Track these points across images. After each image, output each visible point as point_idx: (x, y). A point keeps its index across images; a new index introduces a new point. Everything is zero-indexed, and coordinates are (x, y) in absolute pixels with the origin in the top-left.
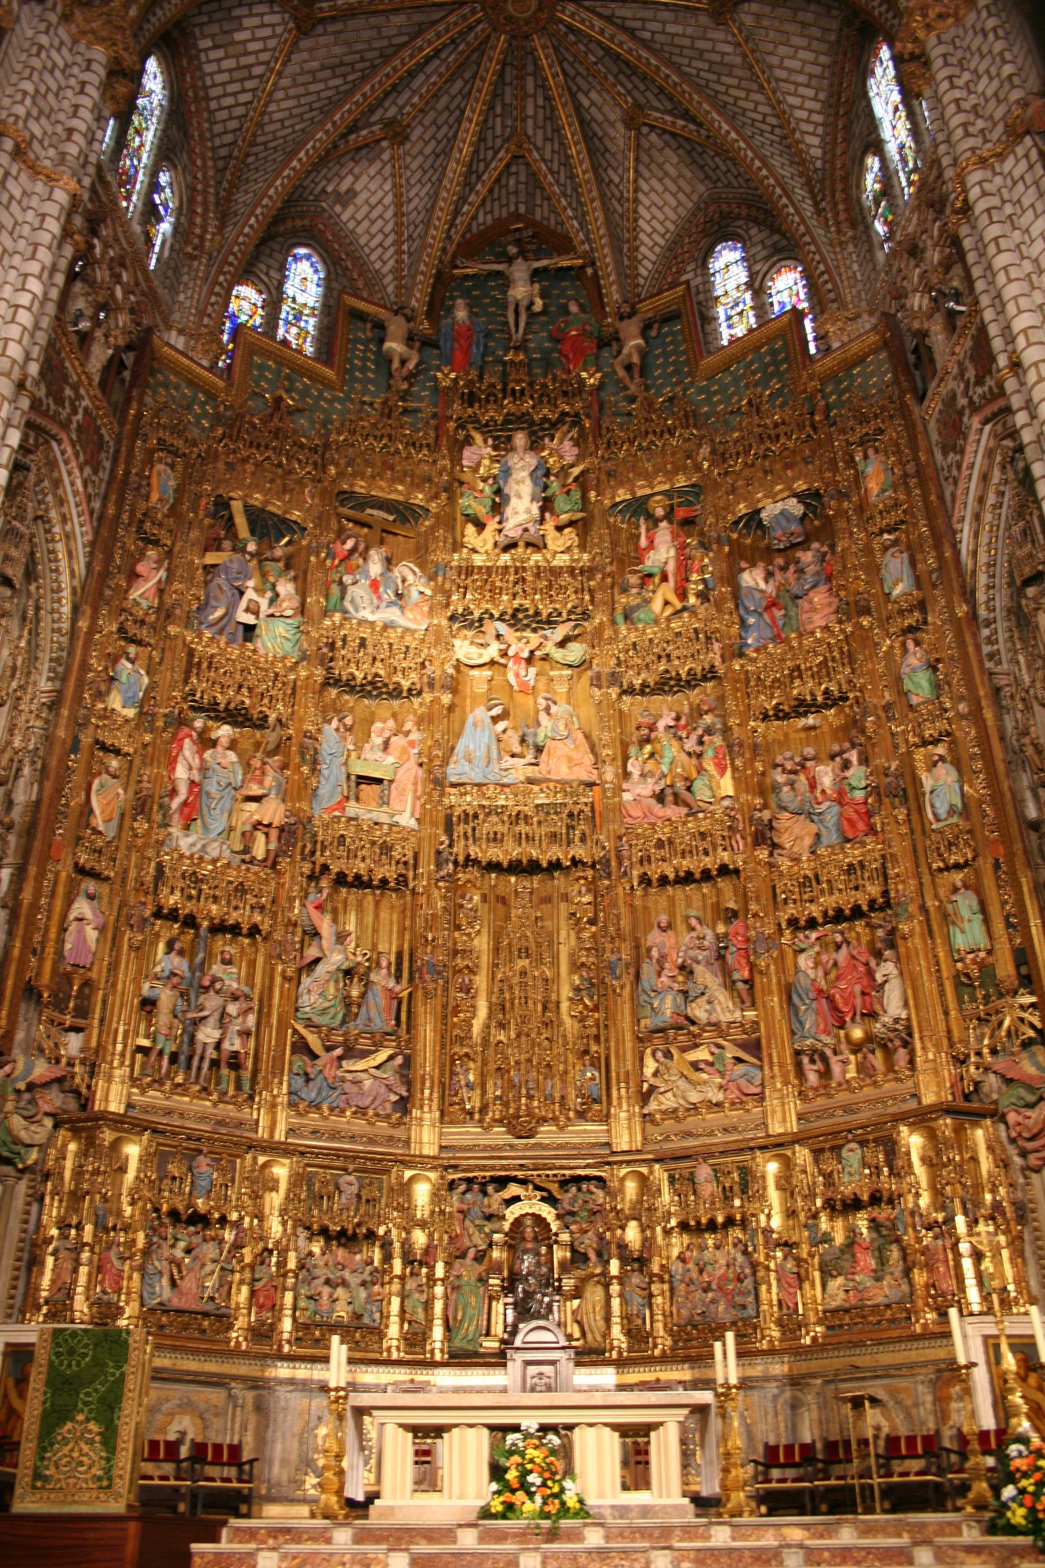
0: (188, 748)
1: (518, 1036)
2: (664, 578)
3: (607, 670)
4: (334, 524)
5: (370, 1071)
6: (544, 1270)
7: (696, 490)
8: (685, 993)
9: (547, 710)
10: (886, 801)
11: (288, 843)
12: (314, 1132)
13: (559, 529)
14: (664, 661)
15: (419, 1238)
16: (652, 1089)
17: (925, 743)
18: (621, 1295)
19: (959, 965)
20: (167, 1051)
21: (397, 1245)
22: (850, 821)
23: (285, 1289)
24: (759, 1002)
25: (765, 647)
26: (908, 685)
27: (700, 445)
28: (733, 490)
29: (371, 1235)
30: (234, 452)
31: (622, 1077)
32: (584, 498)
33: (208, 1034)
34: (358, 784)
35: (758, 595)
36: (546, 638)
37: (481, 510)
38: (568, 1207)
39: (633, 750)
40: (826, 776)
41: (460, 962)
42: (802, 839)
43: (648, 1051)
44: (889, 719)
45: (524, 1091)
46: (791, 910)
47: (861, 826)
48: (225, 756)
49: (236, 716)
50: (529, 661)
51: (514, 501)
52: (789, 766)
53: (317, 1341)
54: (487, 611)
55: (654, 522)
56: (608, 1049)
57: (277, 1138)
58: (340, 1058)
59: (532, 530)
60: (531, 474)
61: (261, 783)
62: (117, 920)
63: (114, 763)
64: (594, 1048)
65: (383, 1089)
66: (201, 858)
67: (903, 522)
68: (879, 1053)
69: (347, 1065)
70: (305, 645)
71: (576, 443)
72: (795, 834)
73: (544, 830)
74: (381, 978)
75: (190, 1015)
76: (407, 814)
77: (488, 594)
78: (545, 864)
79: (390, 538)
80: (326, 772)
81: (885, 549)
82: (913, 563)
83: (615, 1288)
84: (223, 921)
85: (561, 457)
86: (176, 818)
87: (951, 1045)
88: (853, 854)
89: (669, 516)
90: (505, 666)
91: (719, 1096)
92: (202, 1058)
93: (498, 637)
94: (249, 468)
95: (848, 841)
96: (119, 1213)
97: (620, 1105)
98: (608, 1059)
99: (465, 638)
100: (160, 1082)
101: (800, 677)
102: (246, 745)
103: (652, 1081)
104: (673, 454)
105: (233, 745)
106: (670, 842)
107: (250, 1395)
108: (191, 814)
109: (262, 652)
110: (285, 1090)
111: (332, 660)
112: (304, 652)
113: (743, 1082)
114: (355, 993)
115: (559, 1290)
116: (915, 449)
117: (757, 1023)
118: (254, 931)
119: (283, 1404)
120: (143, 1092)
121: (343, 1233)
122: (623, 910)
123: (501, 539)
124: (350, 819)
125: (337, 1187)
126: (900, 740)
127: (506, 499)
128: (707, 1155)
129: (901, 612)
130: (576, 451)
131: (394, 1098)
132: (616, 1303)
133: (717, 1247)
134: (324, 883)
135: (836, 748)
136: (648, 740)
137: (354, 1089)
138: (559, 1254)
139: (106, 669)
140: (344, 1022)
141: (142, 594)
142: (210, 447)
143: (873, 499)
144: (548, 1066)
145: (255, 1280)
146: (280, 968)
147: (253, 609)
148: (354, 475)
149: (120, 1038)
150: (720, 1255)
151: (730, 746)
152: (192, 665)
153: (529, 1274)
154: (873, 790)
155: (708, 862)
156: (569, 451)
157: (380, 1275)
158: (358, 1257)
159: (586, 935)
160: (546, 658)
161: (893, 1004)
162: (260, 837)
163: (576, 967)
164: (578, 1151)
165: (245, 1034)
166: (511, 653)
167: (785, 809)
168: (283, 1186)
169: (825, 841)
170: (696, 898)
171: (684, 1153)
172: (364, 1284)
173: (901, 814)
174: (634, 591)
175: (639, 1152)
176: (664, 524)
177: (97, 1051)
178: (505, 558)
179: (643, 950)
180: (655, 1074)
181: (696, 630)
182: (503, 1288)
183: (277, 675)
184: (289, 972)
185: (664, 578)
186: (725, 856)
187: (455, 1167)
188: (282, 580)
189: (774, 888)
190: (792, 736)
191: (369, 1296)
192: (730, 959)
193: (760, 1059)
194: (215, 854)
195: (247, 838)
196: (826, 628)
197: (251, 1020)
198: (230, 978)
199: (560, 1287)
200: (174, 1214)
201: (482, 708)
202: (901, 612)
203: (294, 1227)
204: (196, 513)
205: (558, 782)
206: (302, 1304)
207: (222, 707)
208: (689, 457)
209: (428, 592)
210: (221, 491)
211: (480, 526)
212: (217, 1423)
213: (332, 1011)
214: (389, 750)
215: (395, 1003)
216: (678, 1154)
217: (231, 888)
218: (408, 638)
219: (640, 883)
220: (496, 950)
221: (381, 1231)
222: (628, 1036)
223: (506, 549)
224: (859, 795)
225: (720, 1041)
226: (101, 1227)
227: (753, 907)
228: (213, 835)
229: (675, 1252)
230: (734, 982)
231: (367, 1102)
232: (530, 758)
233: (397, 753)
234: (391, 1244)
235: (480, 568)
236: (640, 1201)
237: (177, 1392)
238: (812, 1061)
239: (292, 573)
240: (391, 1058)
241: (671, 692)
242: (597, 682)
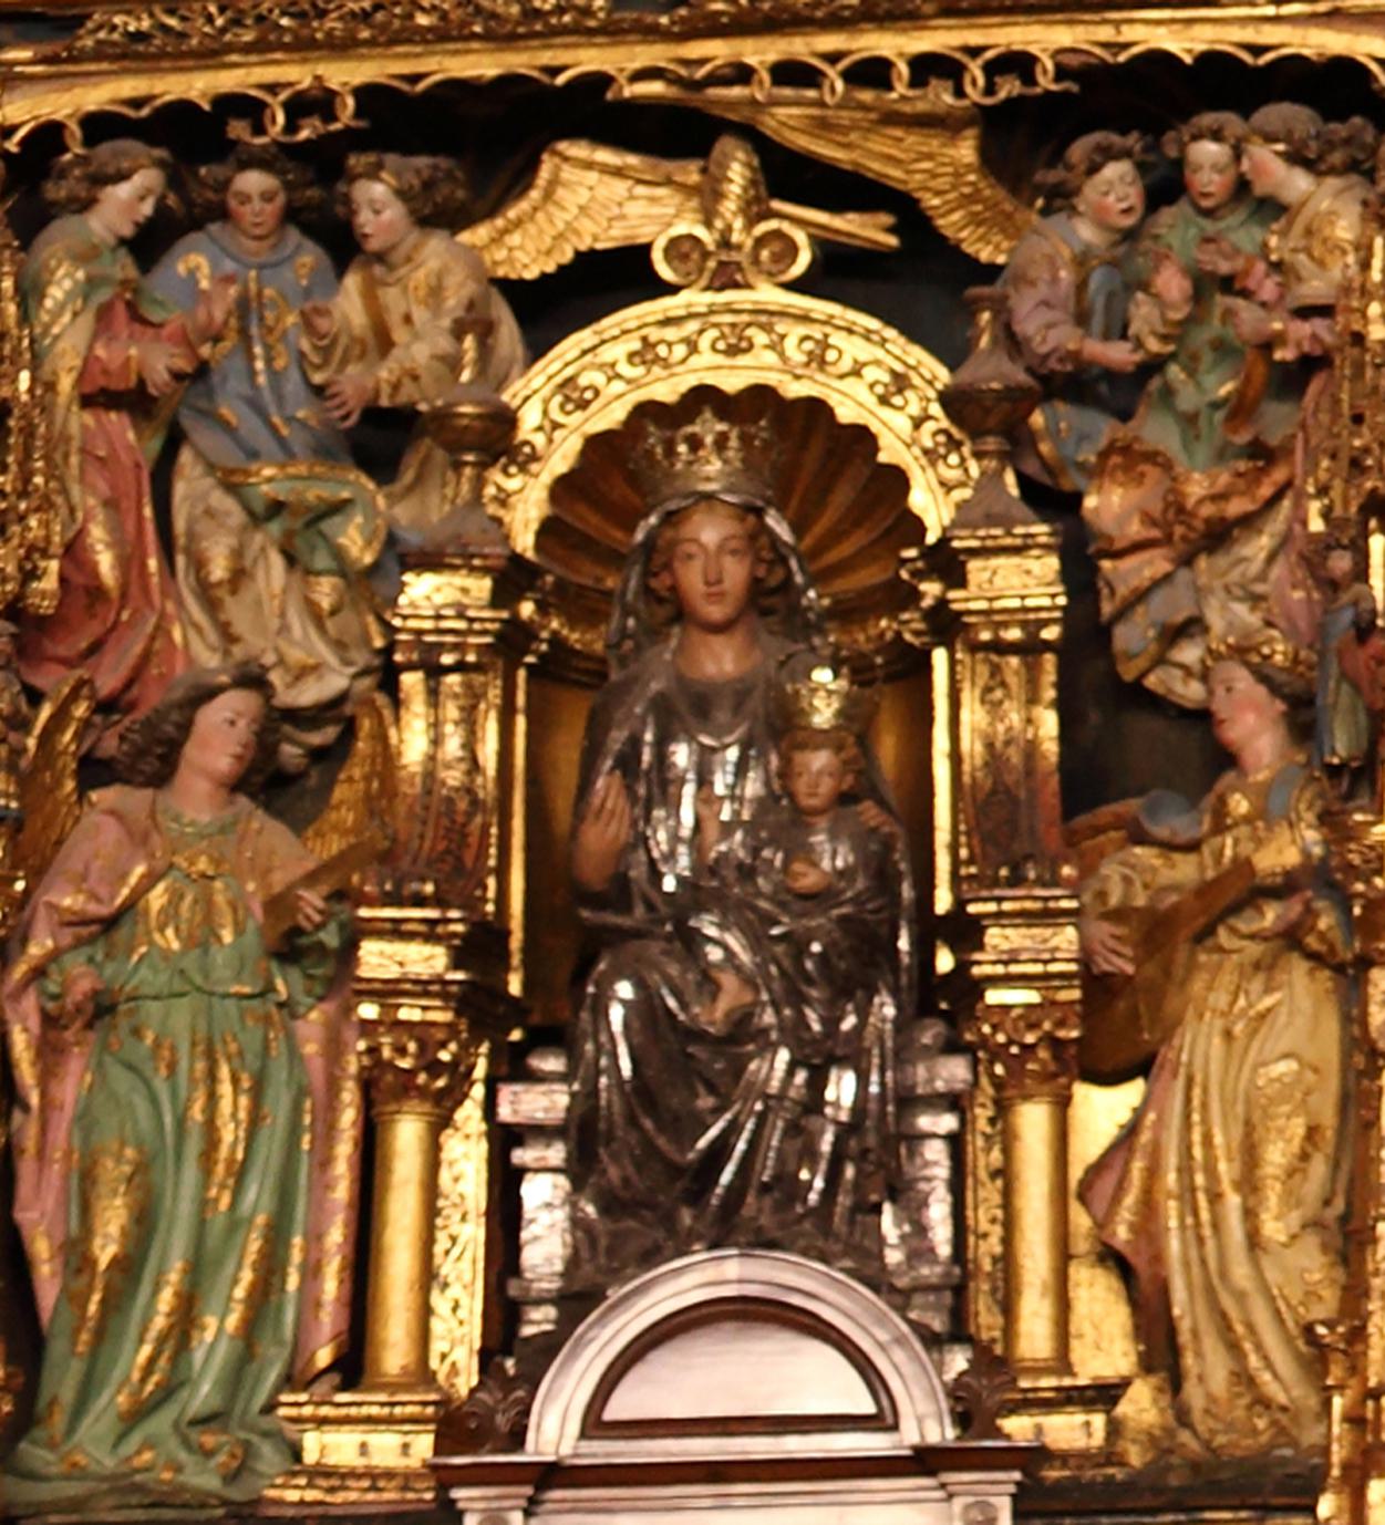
6: (832, 855)
38: (1048, 330)
115: (949, 1004)
182: (479, 1006)
199: (966, 988)
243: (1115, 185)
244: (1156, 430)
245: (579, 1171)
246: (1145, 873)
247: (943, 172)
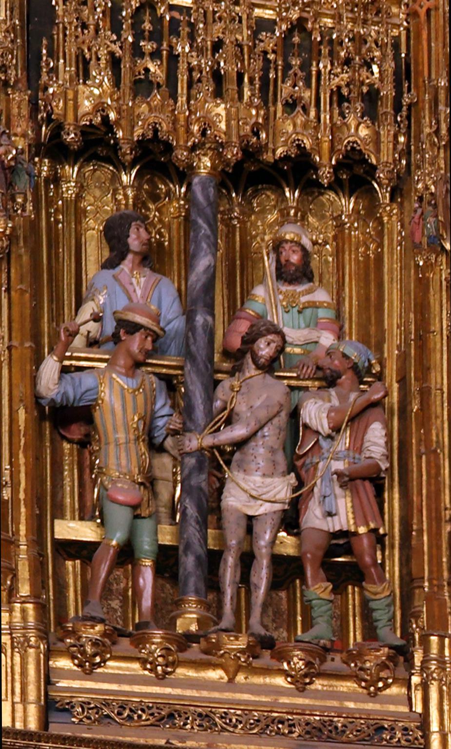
20: (145, 545)
33: (255, 490)
75: (193, 442)
84: (250, 153)
92: (247, 560)
100: (139, 639)
118: (355, 174)
165: (368, 482)
198: (301, 321)
217: (268, 42)
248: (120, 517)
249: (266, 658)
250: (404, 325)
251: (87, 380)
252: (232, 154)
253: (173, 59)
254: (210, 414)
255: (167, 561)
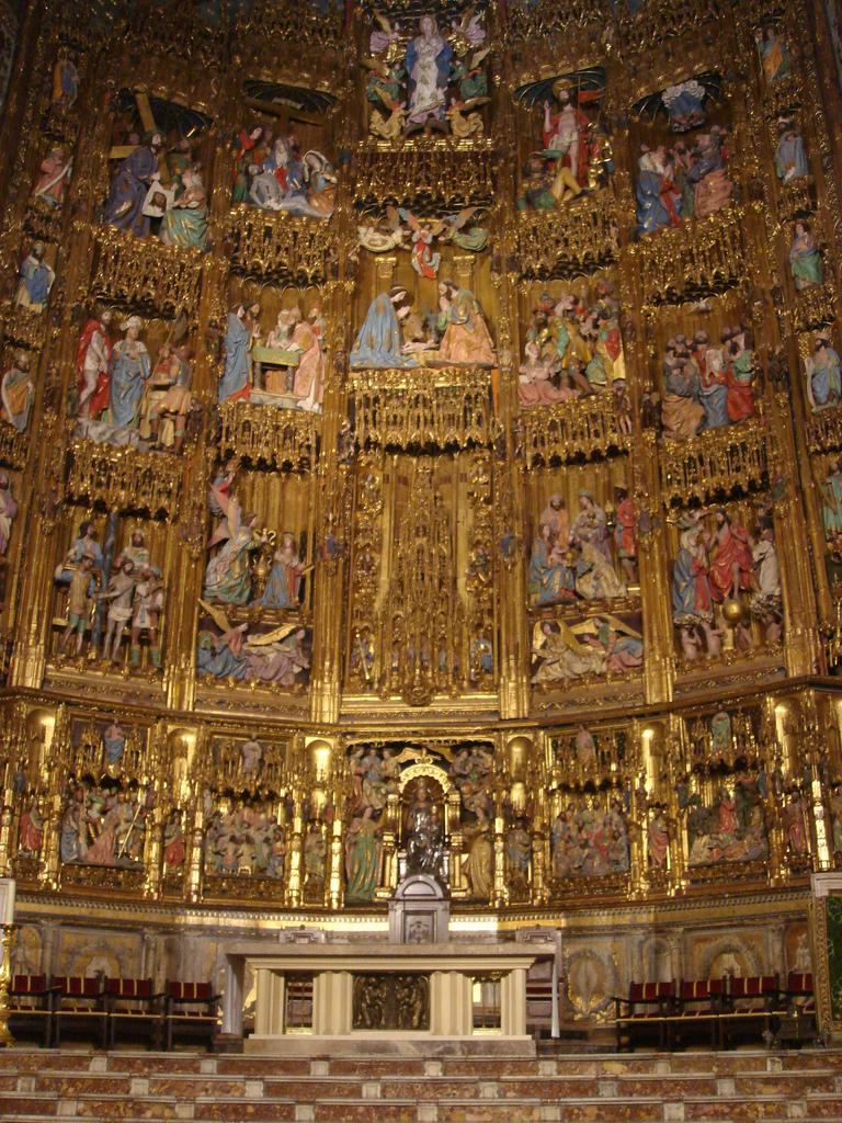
0: (96, 341)
1: (414, 611)
2: (567, 162)
3: (505, 255)
4: (240, 114)
5: (273, 645)
7: (601, 74)
8: (574, 570)
9: (448, 295)
10: (770, 385)
11: (193, 429)
12: (220, 702)
13: (464, 114)
14: (562, 245)
15: (320, 798)
16: (541, 660)
17: (809, 328)
18: (504, 851)
19: (830, 545)
20: (82, 629)
21: (298, 806)
22: (734, 404)
23: (192, 846)
24: (642, 580)
25: (661, 232)
26: (795, 270)
27: (604, 28)
28: (635, 73)
29: (273, 797)
30: (138, 43)
31: (511, 648)
32: (490, 82)
33: (119, 613)
34: (264, 371)
35: (655, 180)
36: (449, 223)
37: (386, 96)
38: (458, 770)
39: (530, 334)
40: (715, 360)
41: (361, 541)
42: (689, 420)
43: (538, 625)
44: (775, 304)
45: (418, 663)
46: (675, 490)
47: (745, 409)
48: (133, 347)
49: (142, 307)
50: (435, 245)
51: (419, 86)
52: (680, 349)
53: (224, 891)
54: (391, 198)
55: (558, 105)
56: (499, 621)
57: (185, 707)
58: (245, 634)
59: (438, 116)
60: (437, 60)
61: (168, 372)
62: (30, 508)
63: (23, 358)
64: (487, 621)
65: (285, 663)
66: (110, 447)
67: (798, 105)
68: (754, 627)
69: (251, 639)
70: (211, 236)
71: (483, 25)
72: (682, 416)
73: (441, 413)
74: (284, 557)
75: (101, 596)
76: (310, 400)
77: (392, 181)
78: (442, 447)
79: (300, 127)
80: (231, 361)
81: (780, 132)
82: (806, 146)
83: (499, 844)
84: (130, 507)
85: (468, 41)
86: (87, 408)
87: (819, 621)
88: (735, 436)
89: (573, 100)
90: (410, 252)
91: (604, 667)
93: (403, 223)
94: (155, 60)
95: (732, 423)
96: (38, 778)
97: (509, 676)
98: (499, 632)
99: (371, 224)
100: (76, 659)
101: (692, 261)
102: (154, 335)
103: (541, 653)
104: (578, 37)
105: (142, 336)
106: (563, 424)
107: (162, 940)
108: (101, 403)
109: (169, 243)
110: (192, 664)
111: (237, 250)
112: (209, 243)
113: (624, 655)
114: (261, 571)
115: (448, 845)
116: (813, 32)
117: (640, 598)
119: (192, 947)
120: (58, 668)
121: (246, 795)
122: (517, 490)
123: (407, 125)
124: (254, 406)
125: (241, 753)
126: (785, 325)
127: (412, 85)
128: (586, 723)
129: (792, 197)
130: (483, 34)
131: (297, 670)
132: (500, 858)
133: (596, 807)
134: (230, 468)
135: (727, 331)
136: (545, 324)
137: (260, 661)
138: (449, 813)
139: (12, 266)
140: (251, 598)
141: (48, 190)
142: (114, 40)
143: (770, 81)
144: (443, 638)
145: (163, 839)
146: (187, 547)
147: (159, 202)
148: (260, 64)
149: (35, 617)
150: (597, 813)
151: (623, 331)
152: (97, 258)
153: (421, 831)
154: (759, 374)
155: (600, 444)
156: (476, 35)
157: (282, 833)
158: (263, 816)
159: (483, 513)
160: (450, 243)
161: (768, 581)
162: (169, 425)
163: (474, 545)
164: (469, 719)
165: (155, 613)
166: (414, 239)
167: (673, 392)
168: (191, 752)
169: (711, 423)
170: (589, 478)
171: (567, 720)
172: (267, 840)
173: (783, 398)
174: (536, 176)
175: (525, 719)
176: (568, 108)
177: (13, 631)
178: (410, 143)
179: (536, 529)
180: (544, 646)
181: (594, 214)
182: (396, 844)
183: (183, 266)
184: (195, 553)
185: (567, 162)
186: (615, 438)
187: (353, 734)
188: (188, 172)
189: (660, 469)
190: (685, 319)
191: (271, 853)
192: (616, 534)
193: (641, 632)
194: (124, 441)
195: (157, 426)
196: (719, 213)
197: (160, 599)
198: (140, 559)
199: (449, 843)
200: (88, 778)
201: (385, 295)
202: (792, 197)
203: (201, 790)
204: (101, 108)
205: (456, 365)
206: (209, 859)
207: (129, 299)
208: (594, 39)
209: (334, 179)
210: (125, 84)
211: (387, 113)
212: (131, 964)
213: (239, 589)
214: (295, 342)
215: (299, 581)
216: (562, 721)
217: (139, 474)
218: (313, 226)
219: (534, 464)
220: (396, 529)
221: (282, 793)
222: (519, 611)
223: (411, 135)
224: (744, 378)
225: (605, 615)
226: (20, 791)
227: (639, 487)
228: (122, 425)
229: (557, 812)
230: (620, 559)
231: (271, 673)
232: (431, 343)
233: (300, 340)
234: (293, 803)
235: (385, 154)
236: (524, 765)
237: (94, 937)
238: (691, 635)
239: (199, 165)
240: (293, 632)
241: (570, 276)
242: (497, 267)
243: (465, 754)
244: (469, 781)
245: (407, 862)
246: (469, 830)
247: (446, 752)
248: (75, 618)
249: (116, 669)
250: (172, 562)
251: (71, 574)
252: (125, 506)
253: (110, 477)
254: (108, 588)
255: (88, 636)
